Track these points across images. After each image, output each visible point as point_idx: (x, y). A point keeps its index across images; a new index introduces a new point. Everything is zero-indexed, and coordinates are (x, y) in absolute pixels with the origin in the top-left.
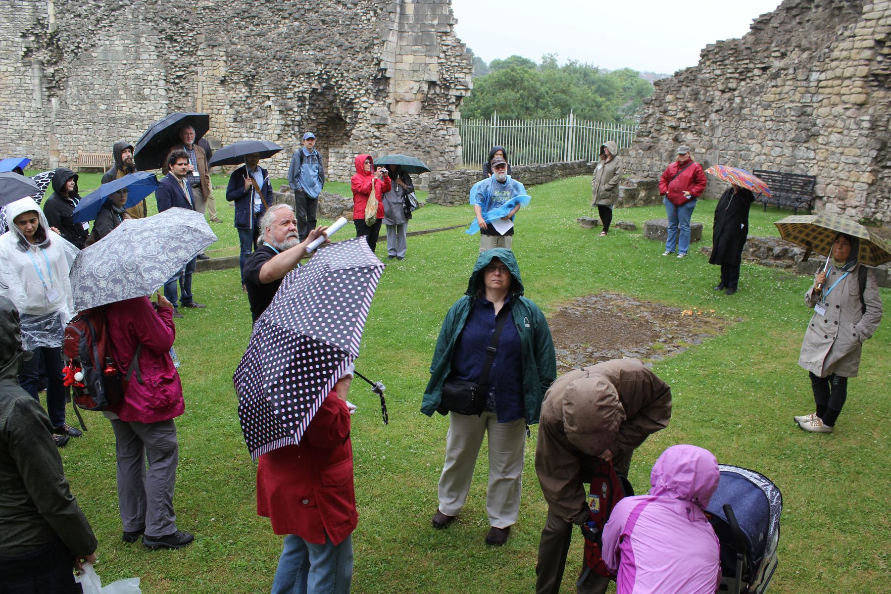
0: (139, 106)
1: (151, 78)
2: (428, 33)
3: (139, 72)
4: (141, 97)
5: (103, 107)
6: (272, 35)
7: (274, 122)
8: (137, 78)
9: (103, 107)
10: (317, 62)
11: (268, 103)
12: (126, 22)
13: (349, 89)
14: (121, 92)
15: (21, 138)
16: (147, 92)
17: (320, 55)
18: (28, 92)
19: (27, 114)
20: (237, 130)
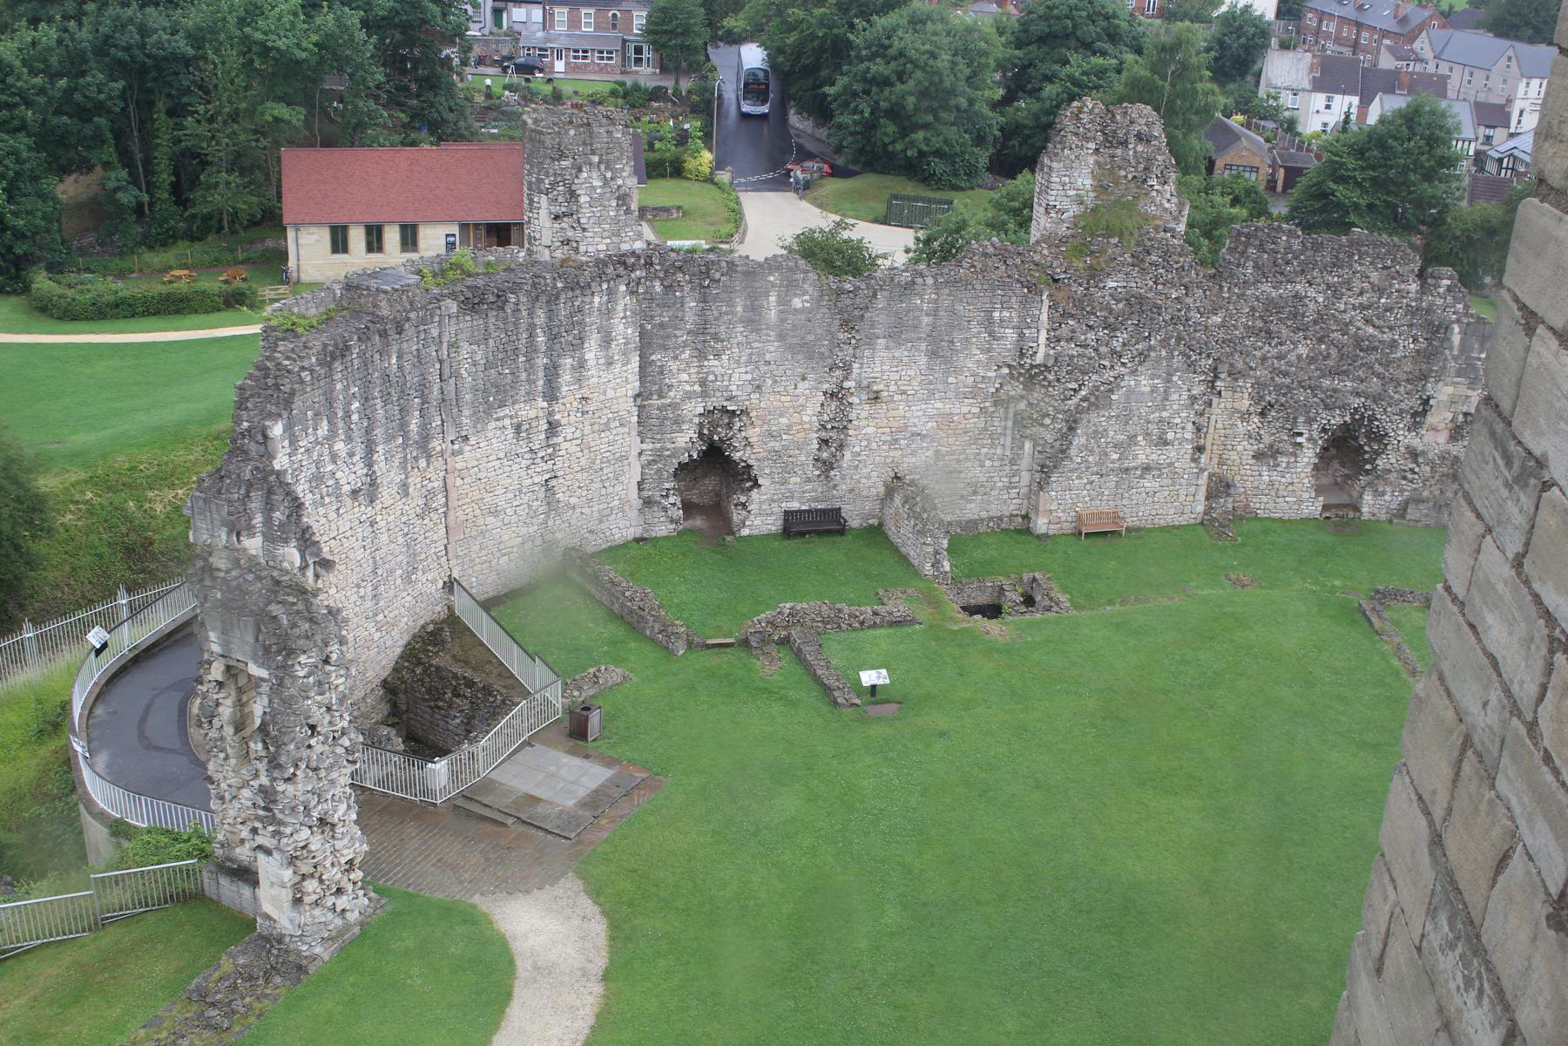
1: (1177, 420)
2: (1475, 369)
3: (1165, 414)
6: (1292, 357)
9: (1115, 456)
10: (1358, 395)
11: (1299, 440)
14: (1140, 438)
15: (975, 493)
16: (1170, 436)
17: (1362, 387)
19: (988, 463)
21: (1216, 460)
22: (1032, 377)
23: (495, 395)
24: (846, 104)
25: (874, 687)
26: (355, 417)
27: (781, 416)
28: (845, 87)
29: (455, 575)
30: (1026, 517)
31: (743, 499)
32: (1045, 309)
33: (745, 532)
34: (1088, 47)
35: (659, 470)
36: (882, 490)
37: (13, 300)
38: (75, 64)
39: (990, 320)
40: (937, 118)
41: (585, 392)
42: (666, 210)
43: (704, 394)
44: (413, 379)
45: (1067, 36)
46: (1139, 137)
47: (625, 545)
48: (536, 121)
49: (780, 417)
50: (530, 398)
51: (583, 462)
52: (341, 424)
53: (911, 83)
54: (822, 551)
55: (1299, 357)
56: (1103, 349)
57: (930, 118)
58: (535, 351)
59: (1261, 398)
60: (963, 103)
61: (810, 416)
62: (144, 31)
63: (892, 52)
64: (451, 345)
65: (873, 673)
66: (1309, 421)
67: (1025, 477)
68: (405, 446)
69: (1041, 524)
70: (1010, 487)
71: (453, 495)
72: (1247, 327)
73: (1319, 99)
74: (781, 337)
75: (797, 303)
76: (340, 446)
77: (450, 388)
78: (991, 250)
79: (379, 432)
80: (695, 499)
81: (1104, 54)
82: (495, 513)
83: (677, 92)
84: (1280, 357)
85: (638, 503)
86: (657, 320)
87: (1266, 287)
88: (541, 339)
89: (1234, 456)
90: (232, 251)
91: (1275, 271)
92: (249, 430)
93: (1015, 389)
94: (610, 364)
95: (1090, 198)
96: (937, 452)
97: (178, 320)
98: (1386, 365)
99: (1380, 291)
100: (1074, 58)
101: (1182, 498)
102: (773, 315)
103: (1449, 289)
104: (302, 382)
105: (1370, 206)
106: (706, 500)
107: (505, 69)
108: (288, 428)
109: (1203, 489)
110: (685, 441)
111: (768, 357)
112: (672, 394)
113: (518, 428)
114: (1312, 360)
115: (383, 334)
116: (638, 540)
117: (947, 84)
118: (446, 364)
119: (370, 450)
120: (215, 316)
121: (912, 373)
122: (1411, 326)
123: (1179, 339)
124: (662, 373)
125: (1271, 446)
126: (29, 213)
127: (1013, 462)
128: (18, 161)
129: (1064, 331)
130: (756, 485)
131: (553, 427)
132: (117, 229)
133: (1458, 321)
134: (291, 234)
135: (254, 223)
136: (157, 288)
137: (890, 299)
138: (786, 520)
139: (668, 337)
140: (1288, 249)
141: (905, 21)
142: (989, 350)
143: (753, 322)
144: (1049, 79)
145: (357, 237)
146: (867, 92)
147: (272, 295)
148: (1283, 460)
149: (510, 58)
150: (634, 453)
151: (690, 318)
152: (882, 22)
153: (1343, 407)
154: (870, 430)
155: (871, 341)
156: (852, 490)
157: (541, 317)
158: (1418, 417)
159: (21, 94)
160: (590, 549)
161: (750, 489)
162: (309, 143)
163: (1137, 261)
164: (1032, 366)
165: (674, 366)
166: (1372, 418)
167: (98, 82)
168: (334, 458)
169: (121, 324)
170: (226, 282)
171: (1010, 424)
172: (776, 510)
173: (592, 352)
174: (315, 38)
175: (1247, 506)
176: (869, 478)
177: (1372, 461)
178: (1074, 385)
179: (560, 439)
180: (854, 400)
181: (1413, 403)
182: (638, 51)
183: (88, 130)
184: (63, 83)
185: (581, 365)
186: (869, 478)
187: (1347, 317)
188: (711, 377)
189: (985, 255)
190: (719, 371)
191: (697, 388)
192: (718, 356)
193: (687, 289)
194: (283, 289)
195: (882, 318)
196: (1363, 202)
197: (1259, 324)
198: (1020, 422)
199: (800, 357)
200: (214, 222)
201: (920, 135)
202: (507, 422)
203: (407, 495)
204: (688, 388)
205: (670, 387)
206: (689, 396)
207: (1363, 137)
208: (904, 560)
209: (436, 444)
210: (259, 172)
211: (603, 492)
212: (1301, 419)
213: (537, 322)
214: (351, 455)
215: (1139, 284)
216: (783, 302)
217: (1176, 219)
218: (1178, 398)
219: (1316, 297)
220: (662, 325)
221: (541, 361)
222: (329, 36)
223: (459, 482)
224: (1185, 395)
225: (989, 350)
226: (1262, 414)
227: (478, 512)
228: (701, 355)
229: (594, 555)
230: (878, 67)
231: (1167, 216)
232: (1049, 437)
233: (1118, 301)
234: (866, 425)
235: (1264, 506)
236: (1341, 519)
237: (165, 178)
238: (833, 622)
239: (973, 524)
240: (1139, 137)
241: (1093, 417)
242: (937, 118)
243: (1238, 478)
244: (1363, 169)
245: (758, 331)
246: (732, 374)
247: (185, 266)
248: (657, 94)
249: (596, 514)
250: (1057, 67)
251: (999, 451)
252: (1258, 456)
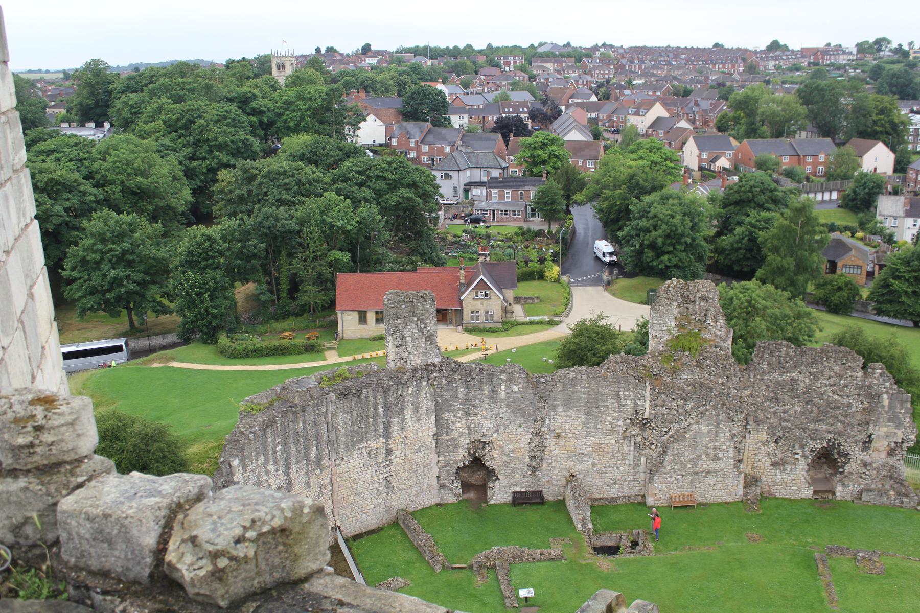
1: (724, 447)
2: (898, 418)
3: (717, 444)
4: (716, 458)
5: (690, 466)
6: (792, 412)
8: (715, 447)
9: (690, 466)
10: (829, 432)
11: (797, 456)
12: (711, 415)
13: (847, 446)
15: (615, 483)
16: (721, 455)
21: (750, 467)
22: (644, 424)
23: (357, 437)
24: (628, 241)
25: (526, 598)
26: (279, 453)
28: (628, 233)
29: (338, 524)
30: (644, 496)
31: (491, 485)
32: (648, 388)
33: (493, 502)
34: (761, 207)
35: (448, 471)
36: (564, 482)
37: (211, 347)
38: (245, 236)
39: (618, 396)
40: (674, 248)
41: (406, 434)
42: (532, 299)
43: (469, 434)
44: (312, 432)
45: (750, 201)
46: (702, 299)
47: (430, 508)
48: (388, 300)
49: (509, 446)
50: (376, 438)
51: (406, 467)
52: (271, 457)
53: (660, 231)
54: (531, 514)
55: (796, 412)
56: (681, 411)
57: (671, 249)
58: (378, 415)
59: (774, 434)
60: (689, 240)
61: (524, 444)
62: (277, 220)
63: (650, 215)
64: (332, 415)
65: (526, 590)
66: (802, 447)
67: (642, 475)
68: (307, 464)
69: (650, 501)
70: (634, 481)
71: (336, 485)
72: (764, 396)
73: (910, 221)
74: (508, 405)
75: (515, 389)
76: (271, 467)
77: (333, 435)
78: (619, 360)
79: (293, 459)
80: (473, 482)
81: (768, 210)
82: (359, 494)
83: (550, 232)
84: (784, 412)
85: (437, 486)
86: (444, 398)
87: (776, 375)
88: (381, 410)
89: (760, 465)
90: (314, 322)
91: (781, 367)
92: (224, 462)
93: (635, 430)
94: (419, 420)
95: (675, 331)
96: (593, 463)
97: (283, 359)
98: (846, 416)
99: (841, 377)
100: (753, 213)
101: (730, 487)
102: (503, 394)
103: (881, 375)
104: (249, 439)
105: (914, 292)
106: (479, 483)
107: (466, 221)
108: (242, 461)
109: (742, 483)
110: (461, 456)
111: (501, 415)
113: (370, 453)
114: (803, 413)
115: (294, 413)
116: (437, 505)
117: (680, 231)
118: (330, 424)
119: (288, 467)
120: (300, 357)
122: (859, 395)
123: (724, 404)
125: (782, 459)
126: (219, 306)
127: (635, 468)
128: (216, 283)
129: (659, 401)
130: (498, 479)
131: (389, 452)
132: (265, 312)
133: (887, 392)
134: (339, 315)
135: (323, 308)
136: (275, 343)
137: (564, 386)
138: (513, 497)
139: (450, 406)
140: (787, 354)
141: (658, 199)
142: (618, 412)
143: (493, 397)
144: (739, 224)
145: (371, 316)
146: (638, 236)
147: (328, 346)
148: (788, 467)
149: (469, 215)
150: (435, 462)
151: (461, 397)
152: (647, 199)
153: (822, 439)
154: (556, 452)
155: (554, 407)
157: (380, 399)
158: (867, 443)
159: (218, 251)
160: (411, 510)
161: (495, 480)
162: (352, 270)
163: (699, 364)
164: (643, 419)
165: (453, 420)
166: (839, 445)
167: (257, 245)
168: (267, 473)
169: (256, 360)
170: (309, 339)
171: (632, 448)
172: (508, 491)
173: (409, 415)
174: (357, 219)
175: (769, 491)
176: (557, 475)
177: (842, 467)
179: (393, 457)
181: (863, 437)
182: (533, 210)
183: (249, 266)
184: (239, 245)
185: (404, 420)
187: (822, 390)
189: (616, 362)
190: (476, 422)
191: (466, 430)
192: (476, 415)
193: (459, 383)
194: (333, 343)
195: (560, 396)
196: (910, 290)
197: (772, 395)
198: (638, 447)
199: (518, 415)
200: (307, 307)
201: (666, 257)
202: (364, 450)
203: (309, 487)
205: (452, 430)
206: (461, 434)
207: (909, 254)
208: (571, 520)
209: (326, 462)
210: (327, 284)
212: (797, 446)
213: (378, 402)
214: (277, 471)
215: (700, 376)
216: (508, 388)
217: (724, 340)
218: (724, 435)
219: (804, 380)
220: (447, 400)
221: (381, 420)
222: (364, 218)
223: (339, 479)
224: (728, 434)
225: (618, 412)
226: (776, 442)
227: (349, 493)
229: (412, 514)
230: (643, 223)
231: (718, 339)
232: (654, 455)
233: (688, 386)
235: (780, 492)
236: (823, 499)
237: (285, 286)
238: (519, 557)
239: (614, 499)
240: (702, 299)
241: (676, 446)
242: (674, 248)
243: (763, 476)
244: (910, 272)
245: (496, 403)
246: (483, 424)
247: (291, 330)
248: (539, 233)
250: (743, 218)
251: (627, 462)
252: (774, 464)
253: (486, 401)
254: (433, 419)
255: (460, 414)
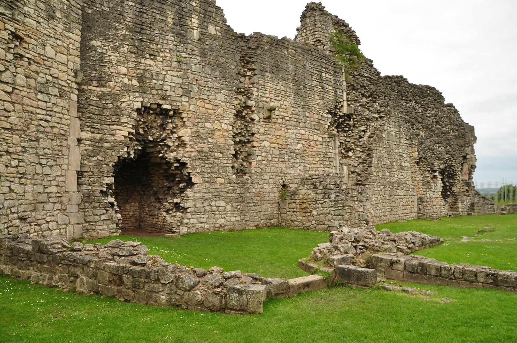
0: (401, 174)
7: (439, 184)
18: (331, 159)
20: (424, 190)
27: (207, 121)
33: (184, 230)
35: (99, 164)
39: (321, 76)
43: (142, 90)
74: (203, 54)
85: (76, 197)
112: (112, 84)
121: (286, 103)
124: (101, 60)
130: (190, 184)
139: (109, 27)
143: (182, 36)
151: (129, 16)
154: (266, 144)
155: (263, 70)
156: (258, 194)
164: (341, 117)
165: (114, 57)
178: (363, 128)
180: (255, 116)
186: (268, 184)
188: (148, 75)
191: (135, 82)
199: (217, 73)
204: (126, 81)
206: (127, 89)
211: (38, 168)
216: (202, 26)
228: (139, 51)
234: (264, 141)
249: (29, 196)
253: (170, 37)
254: (76, 36)
255: (125, 49)
